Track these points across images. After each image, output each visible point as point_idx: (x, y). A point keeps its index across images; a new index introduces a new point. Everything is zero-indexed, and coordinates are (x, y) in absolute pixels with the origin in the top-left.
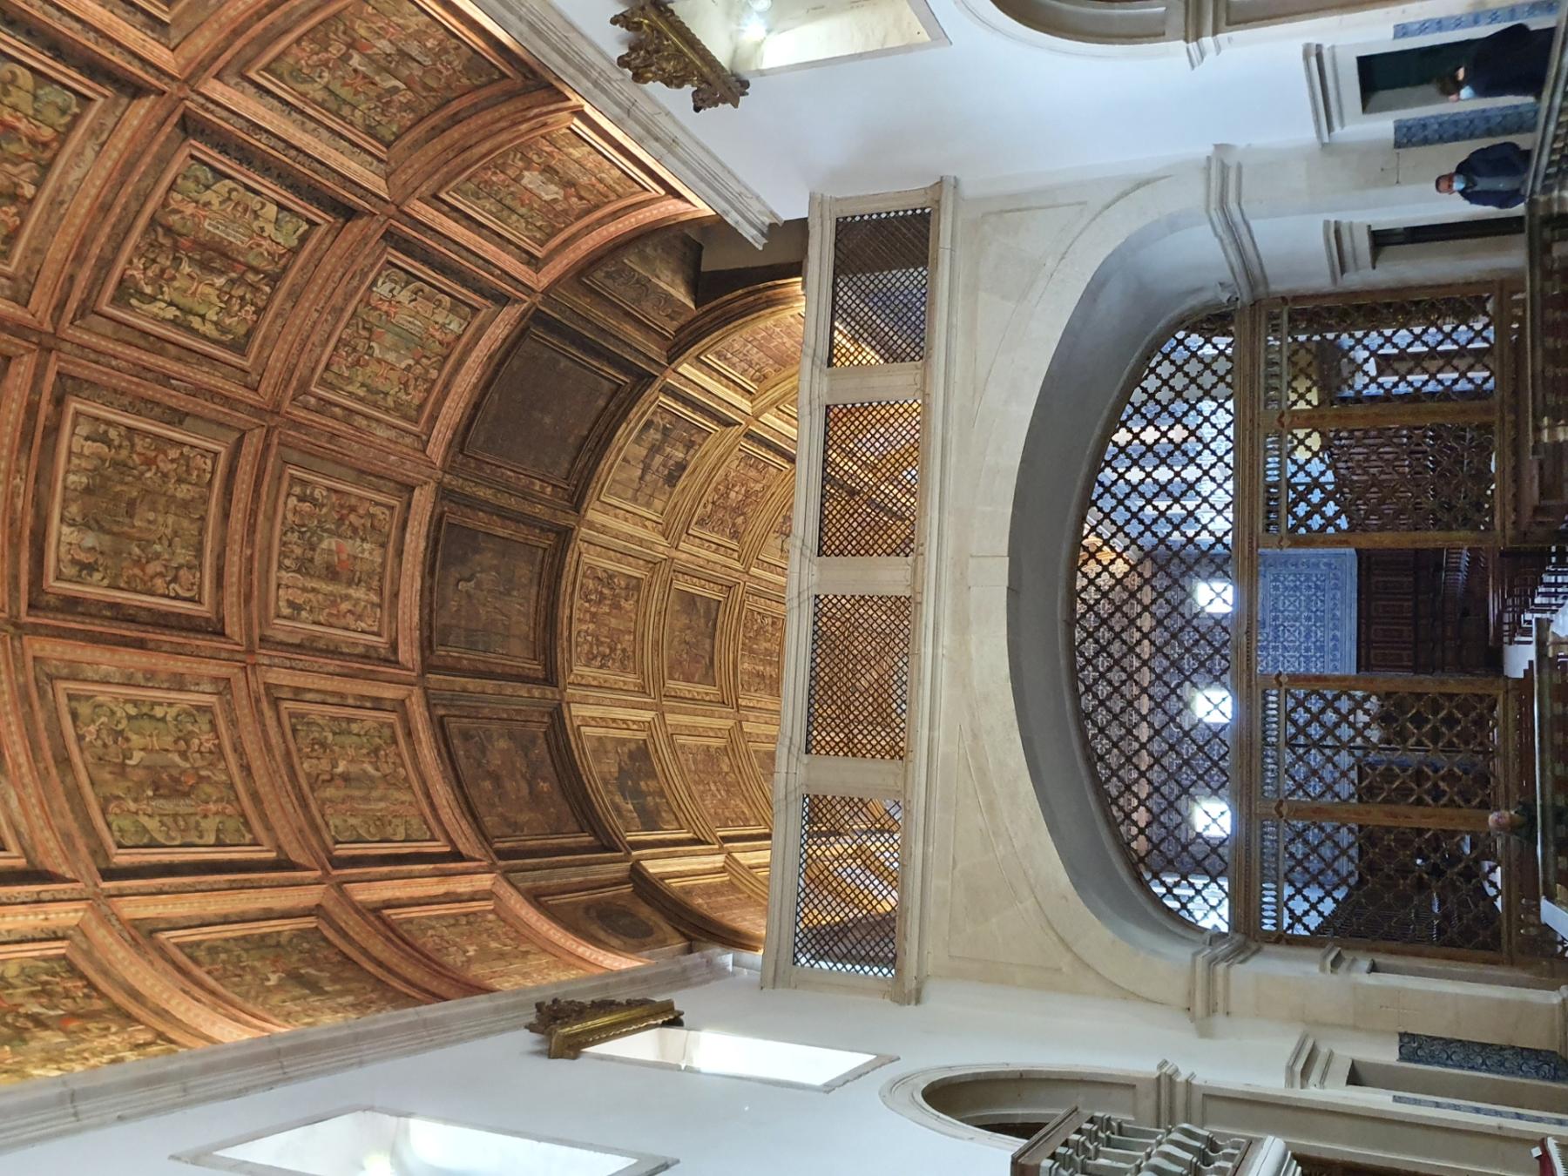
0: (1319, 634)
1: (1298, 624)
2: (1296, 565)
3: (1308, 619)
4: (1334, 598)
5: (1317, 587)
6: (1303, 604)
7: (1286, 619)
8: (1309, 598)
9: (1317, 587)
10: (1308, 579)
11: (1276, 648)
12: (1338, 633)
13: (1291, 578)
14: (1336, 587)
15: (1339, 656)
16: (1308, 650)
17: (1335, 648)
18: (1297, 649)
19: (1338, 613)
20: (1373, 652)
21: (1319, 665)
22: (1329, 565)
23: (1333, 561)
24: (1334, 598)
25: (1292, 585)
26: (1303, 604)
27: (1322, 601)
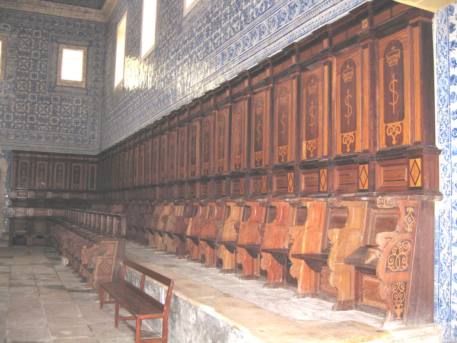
0: (43, 127)
1: (51, 113)
4: (69, 139)
5: (77, 128)
7: (55, 106)
9: (77, 128)
10: (83, 122)
11: (33, 97)
12: (43, 140)
13: (84, 112)
16: (32, 119)
17: (32, 137)
18: (32, 112)
19: (58, 141)
21: (20, 126)
23: (95, 140)
24: (69, 139)
27: (67, 131)
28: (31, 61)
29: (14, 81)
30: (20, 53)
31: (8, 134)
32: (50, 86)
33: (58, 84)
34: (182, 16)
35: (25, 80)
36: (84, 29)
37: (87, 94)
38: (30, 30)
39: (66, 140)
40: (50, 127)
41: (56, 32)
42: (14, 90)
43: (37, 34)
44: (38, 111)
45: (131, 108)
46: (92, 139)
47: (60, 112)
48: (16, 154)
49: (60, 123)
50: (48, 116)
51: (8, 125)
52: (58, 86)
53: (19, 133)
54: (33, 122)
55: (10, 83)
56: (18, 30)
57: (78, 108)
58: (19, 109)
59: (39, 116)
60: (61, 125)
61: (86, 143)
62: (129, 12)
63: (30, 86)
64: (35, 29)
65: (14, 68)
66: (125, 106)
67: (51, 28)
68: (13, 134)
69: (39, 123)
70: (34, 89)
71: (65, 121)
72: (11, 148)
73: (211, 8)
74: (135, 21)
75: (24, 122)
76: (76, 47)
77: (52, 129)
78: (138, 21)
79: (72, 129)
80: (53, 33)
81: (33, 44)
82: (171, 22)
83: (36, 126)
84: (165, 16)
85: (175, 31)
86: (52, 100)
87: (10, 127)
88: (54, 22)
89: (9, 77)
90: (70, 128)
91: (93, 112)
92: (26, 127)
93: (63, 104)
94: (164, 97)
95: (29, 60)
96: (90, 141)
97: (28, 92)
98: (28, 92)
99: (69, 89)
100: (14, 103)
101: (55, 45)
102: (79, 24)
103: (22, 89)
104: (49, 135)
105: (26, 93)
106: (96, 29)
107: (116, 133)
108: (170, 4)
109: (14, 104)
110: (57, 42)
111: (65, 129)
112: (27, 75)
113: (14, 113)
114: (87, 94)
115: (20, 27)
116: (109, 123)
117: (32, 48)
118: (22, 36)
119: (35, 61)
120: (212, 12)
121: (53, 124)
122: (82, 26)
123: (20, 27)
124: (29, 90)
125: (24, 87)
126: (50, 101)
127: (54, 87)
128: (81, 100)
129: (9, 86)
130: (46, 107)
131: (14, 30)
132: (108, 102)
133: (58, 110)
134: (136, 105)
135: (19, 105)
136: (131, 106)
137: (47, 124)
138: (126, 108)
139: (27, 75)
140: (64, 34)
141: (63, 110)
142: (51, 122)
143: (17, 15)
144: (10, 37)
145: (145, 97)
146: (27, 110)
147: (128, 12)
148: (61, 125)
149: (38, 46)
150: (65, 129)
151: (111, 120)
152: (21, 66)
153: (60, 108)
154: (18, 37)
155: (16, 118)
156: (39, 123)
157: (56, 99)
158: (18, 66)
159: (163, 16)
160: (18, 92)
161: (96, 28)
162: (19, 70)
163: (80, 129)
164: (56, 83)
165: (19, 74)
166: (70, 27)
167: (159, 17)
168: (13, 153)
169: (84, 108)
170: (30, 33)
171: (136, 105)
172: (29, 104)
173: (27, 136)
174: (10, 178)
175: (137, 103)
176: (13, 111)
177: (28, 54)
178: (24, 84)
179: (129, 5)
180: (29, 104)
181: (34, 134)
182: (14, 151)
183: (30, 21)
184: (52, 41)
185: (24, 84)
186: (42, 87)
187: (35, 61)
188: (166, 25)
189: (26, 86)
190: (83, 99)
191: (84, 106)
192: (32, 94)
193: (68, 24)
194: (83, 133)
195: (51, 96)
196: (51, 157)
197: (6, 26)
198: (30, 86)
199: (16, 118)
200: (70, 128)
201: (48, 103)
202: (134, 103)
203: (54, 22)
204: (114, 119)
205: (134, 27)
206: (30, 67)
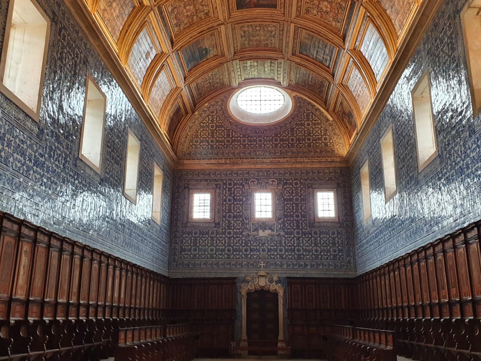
0: (308, 257)
1: (313, 245)
2: (348, 244)
3: (316, 251)
6: (325, 248)
8: (329, 251)
10: (339, 250)
12: (309, 267)
14: (336, 266)
15: (296, 267)
16: (299, 250)
18: (298, 245)
19: (321, 267)
20: (299, 286)
21: (290, 257)
22: (349, 262)
24: (329, 265)
25: (336, 242)
26: (325, 248)
27: (327, 258)
28: (294, 205)
29: (283, 222)
30: (285, 200)
31: (282, 265)
32: (310, 223)
33: (316, 221)
34: (418, 172)
35: (291, 220)
36: (332, 174)
37: (340, 227)
38: (291, 181)
39: (327, 266)
40: (313, 256)
41: (310, 180)
42: (283, 229)
43: (296, 184)
44: (303, 243)
45: (382, 240)
46: (348, 264)
47: (320, 244)
48: (289, 280)
49: (321, 253)
50: (311, 247)
51: (281, 256)
52: (317, 222)
53: (289, 263)
54: (300, 253)
55: (280, 224)
56: (282, 183)
57: (334, 239)
58: (288, 243)
59: (304, 247)
60: (322, 254)
61: (344, 268)
62: (370, 161)
63: (295, 225)
64: (294, 180)
65: (282, 212)
66: (376, 237)
67: (306, 178)
68: (285, 264)
69: (305, 253)
70: (298, 226)
71: (325, 250)
72: (285, 276)
73: (441, 170)
74: (376, 169)
75: (293, 254)
76: (328, 189)
77: (315, 258)
78: (379, 170)
79: (331, 256)
80: (308, 182)
81: (294, 192)
82: (408, 175)
83: (302, 256)
84: (403, 169)
85: (413, 182)
86: (313, 234)
87: (283, 258)
88: (308, 173)
89: (279, 219)
90: (330, 256)
91: (347, 240)
92: (295, 257)
93: (321, 236)
94: (410, 233)
95: (292, 204)
96: (347, 266)
97: (294, 230)
98: (294, 230)
99: (325, 224)
100: (284, 238)
101: (311, 190)
102: (327, 171)
103: (289, 227)
104: (313, 263)
105: (292, 230)
106: (342, 174)
107: (370, 259)
108: (406, 161)
109: (285, 240)
110: (312, 187)
111: (326, 257)
112: (291, 216)
113: (284, 247)
114: (340, 227)
115: (283, 181)
116: (362, 250)
117: (294, 195)
118: (285, 187)
119: (297, 205)
120: (442, 172)
121: (316, 253)
122: (330, 173)
123: (283, 181)
124: (295, 227)
125: (291, 226)
126: (311, 235)
127: (313, 223)
128: (336, 232)
129: (279, 226)
130: (309, 240)
131: (280, 183)
132: (359, 232)
133: (318, 241)
134: (386, 237)
135: (288, 240)
136: (382, 238)
137: (311, 254)
138: (377, 239)
139: (291, 216)
140: (317, 180)
141: (322, 242)
142: (314, 252)
143: (281, 171)
144: (277, 188)
145: (393, 231)
146: (294, 243)
147: (369, 161)
148: (322, 254)
149: (298, 193)
150: (326, 257)
151: (364, 248)
152: (287, 209)
153: (320, 240)
154: (283, 188)
155: (286, 250)
156: (305, 253)
157: (315, 233)
158: (284, 210)
159: (401, 169)
160: (286, 230)
161: (341, 172)
162: (285, 213)
163: (338, 256)
164: (314, 220)
165: (286, 216)
166: (320, 175)
167: (398, 169)
168: (287, 280)
169: (339, 239)
170: (291, 184)
171: (386, 237)
172: (295, 239)
173: (296, 265)
174: (286, 300)
175: (387, 236)
176: (284, 245)
177: (291, 200)
178: (290, 223)
179: (369, 155)
180: (295, 239)
181: (302, 263)
182: (288, 278)
183: (290, 175)
184: (308, 188)
185: (290, 223)
186: (304, 225)
187: (297, 205)
188: (404, 177)
189: (292, 225)
190: (337, 231)
191: (339, 236)
192: (297, 231)
193: (319, 172)
194: (341, 259)
195: (311, 231)
196: (317, 281)
197: (273, 181)
198: (295, 225)
199: (286, 250)
200: (330, 256)
201: (310, 236)
202: (385, 235)
203: (308, 173)
204: (367, 248)
205: (376, 174)
206: (293, 210)
